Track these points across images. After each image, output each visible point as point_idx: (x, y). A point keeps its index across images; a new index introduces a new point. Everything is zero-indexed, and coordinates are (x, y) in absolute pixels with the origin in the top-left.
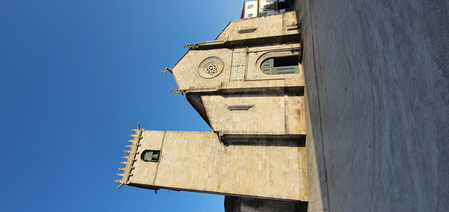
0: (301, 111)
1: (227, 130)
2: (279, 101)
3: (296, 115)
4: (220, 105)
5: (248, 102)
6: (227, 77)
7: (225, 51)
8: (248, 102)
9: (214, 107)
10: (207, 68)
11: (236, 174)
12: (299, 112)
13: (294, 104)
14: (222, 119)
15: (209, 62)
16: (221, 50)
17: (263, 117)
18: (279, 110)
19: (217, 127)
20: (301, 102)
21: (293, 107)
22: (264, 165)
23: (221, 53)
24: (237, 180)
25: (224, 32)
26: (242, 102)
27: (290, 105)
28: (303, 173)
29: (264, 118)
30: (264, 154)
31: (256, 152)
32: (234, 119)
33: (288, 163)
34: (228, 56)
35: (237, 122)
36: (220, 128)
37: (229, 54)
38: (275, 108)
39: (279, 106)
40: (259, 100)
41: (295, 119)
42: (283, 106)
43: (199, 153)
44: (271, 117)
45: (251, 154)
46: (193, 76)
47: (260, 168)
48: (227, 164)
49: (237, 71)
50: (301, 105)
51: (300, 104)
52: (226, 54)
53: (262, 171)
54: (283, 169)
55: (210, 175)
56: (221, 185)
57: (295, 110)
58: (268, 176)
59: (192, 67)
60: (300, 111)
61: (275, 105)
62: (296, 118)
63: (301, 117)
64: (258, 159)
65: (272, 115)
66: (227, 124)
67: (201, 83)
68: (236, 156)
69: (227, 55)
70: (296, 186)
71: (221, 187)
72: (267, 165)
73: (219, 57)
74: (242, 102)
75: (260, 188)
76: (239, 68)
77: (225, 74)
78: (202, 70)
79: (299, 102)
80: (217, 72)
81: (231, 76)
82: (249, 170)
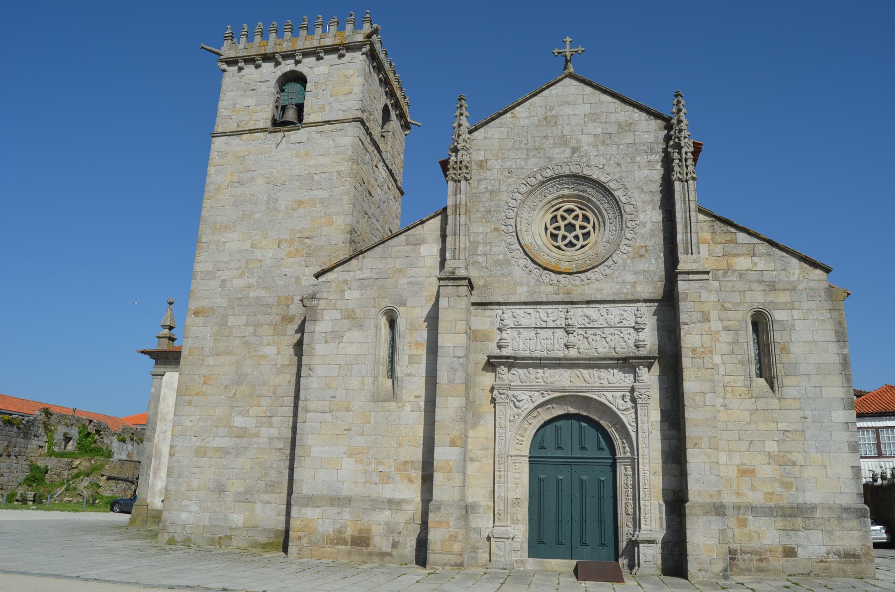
0: (364, 549)
1: (319, 316)
2: (406, 481)
3: (350, 532)
4: (403, 281)
5: (409, 375)
6: (520, 290)
7: (652, 268)
8: (409, 375)
9: (399, 263)
10: (581, 209)
11: (226, 354)
12: (361, 543)
13: (390, 529)
14: (353, 295)
15: (605, 213)
16: (658, 248)
17: (353, 428)
18: (375, 477)
19: (329, 284)
20: (394, 552)
21: (379, 527)
22: (242, 433)
23: (643, 252)
24: (211, 361)
25: (763, 247)
26: (411, 356)
27: (386, 515)
28: (220, 538)
29: (349, 430)
30: (274, 432)
31: (280, 408)
32: (356, 334)
33: (246, 498)
34: (624, 282)
35: (341, 345)
36: (325, 295)
37: (634, 284)
38: (381, 468)
39: (385, 478)
40: (415, 413)
41: (337, 526)
42: (388, 492)
43: (286, 240)
44: (352, 453)
45: (274, 393)
46: (533, 164)
47: (238, 421)
48: (251, 329)
49: (544, 325)
50: (385, 549)
51: (389, 550)
52: (636, 273)
53: (230, 427)
54: (232, 484)
55: (228, 284)
56: (201, 318)
57: (368, 531)
58: (219, 442)
59: (574, 150)
60: (362, 546)
61: (391, 467)
62: (339, 531)
63: (343, 547)
64: (261, 414)
65: (360, 456)
66: (337, 315)
67: (499, 200)
68: (270, 350)
69: (629, 277)
70: (191, 516)
71: (200, 320)
72: (243, 442)
73: (623, 248)
74: (411, 356)
75: (191, 421)
76: (561, 333)
77: (532, 282)
78: (567, 192)
79: (395, 545)
80: (559, 248)
81: (524, 307)
82: (233, 392)
